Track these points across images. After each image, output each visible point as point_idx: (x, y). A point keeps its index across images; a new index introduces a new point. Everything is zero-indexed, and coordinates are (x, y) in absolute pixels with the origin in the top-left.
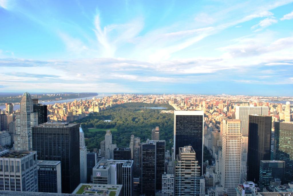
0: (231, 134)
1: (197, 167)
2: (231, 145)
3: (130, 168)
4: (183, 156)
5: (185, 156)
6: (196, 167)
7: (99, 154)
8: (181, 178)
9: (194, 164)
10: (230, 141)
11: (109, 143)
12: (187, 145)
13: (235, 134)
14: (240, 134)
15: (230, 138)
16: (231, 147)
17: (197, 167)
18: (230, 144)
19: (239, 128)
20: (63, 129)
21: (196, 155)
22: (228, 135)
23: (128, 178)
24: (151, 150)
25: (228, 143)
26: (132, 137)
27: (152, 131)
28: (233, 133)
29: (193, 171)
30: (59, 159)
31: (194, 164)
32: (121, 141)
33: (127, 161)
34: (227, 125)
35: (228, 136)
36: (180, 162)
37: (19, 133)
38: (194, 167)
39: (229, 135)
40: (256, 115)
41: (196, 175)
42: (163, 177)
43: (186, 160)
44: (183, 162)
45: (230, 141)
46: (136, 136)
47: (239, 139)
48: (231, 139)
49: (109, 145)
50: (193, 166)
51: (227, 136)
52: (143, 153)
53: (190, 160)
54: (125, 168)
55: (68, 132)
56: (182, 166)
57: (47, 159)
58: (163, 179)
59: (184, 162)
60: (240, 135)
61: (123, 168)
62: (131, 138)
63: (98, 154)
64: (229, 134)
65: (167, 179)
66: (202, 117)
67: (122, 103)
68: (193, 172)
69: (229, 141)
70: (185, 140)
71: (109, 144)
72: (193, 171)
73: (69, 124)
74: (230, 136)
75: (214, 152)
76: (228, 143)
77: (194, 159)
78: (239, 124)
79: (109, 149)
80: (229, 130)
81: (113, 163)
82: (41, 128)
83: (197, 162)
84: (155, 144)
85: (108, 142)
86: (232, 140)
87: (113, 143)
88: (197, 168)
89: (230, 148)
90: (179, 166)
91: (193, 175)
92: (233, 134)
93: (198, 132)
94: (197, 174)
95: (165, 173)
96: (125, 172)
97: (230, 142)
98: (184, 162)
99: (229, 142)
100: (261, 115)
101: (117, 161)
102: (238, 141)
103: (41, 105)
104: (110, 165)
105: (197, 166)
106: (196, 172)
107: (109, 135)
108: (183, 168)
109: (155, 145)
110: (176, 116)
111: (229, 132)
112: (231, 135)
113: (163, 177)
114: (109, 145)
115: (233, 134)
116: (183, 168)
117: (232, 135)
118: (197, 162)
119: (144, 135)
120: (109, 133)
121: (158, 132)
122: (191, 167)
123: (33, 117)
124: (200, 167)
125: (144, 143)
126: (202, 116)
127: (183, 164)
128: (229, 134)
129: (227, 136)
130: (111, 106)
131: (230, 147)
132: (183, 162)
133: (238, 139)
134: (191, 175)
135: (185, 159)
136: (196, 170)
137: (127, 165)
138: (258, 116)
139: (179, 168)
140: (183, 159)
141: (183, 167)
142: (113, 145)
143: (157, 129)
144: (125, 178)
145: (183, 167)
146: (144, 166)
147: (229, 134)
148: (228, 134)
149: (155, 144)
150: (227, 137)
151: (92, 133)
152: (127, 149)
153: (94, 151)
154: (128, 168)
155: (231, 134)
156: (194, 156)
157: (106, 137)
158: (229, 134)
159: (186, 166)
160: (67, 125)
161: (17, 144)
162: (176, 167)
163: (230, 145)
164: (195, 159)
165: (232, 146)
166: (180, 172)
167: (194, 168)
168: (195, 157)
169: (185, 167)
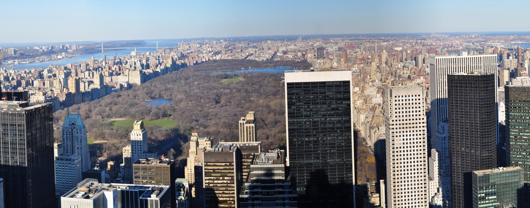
0: (401, 118)
1: (290, 196)
2: (404, 143)
4: (255, 172)
6: (287, 196)
9: (281, 190)
10: (400, 136)
11: (139, 149)
13: (411, 118)
14: (421, 117)
15: (400, 128)
16: (404, 147)
17: (290, 196)
18: (402, 142)
19: (419, 105)
22: (395, 123)
24: (223, 164)
25: (397, 140)
28: (406, 116)
31: (281, 190)
34: (394, 99)
35: (396, 125)
38: (281, 196)
39: (398, 122)
40: (463, 74)
45: (402, 134)
47: (420, 129)
48: (403, 130)
49: (140, 154)
51: (393, 125)
52: (207, 171)
60: (423, 119)
64: (398, 119)
69: (398, 134)
71: (139, 152)
74: (400, 124)
76: (397, 140)
78: (419, 95)
80: (398, 111)
85: (137, 147)
86: (405, 134)
88: (290, 199)
89: (402, 149)
92: (408, 118)
93: (340, 119)
97: (402, 138)
99: (399, 138)
100: (472, 73)
102: (419, 133)
105: (290, 193)
108: (257, 199)
111: (398, 115)
112: (401, 122)
115: (406, 118)
116: (257, 199)
117: (405, 122)
122: (276, 196)
128: (396, 119)
129: (393, 125)
131: (400, 148)
133: (418, 129)
136: (287, 201)
138: (466, 74)
147: (398, 119)
148: (395, 119)
150: (395, 127)
155: (401, 118)
156: (280, 172)
158: (396, 119)
163: (400, 144)
164: (284, 178)
165: (405, 145)
167: (284, 199)
168: (284, 172)
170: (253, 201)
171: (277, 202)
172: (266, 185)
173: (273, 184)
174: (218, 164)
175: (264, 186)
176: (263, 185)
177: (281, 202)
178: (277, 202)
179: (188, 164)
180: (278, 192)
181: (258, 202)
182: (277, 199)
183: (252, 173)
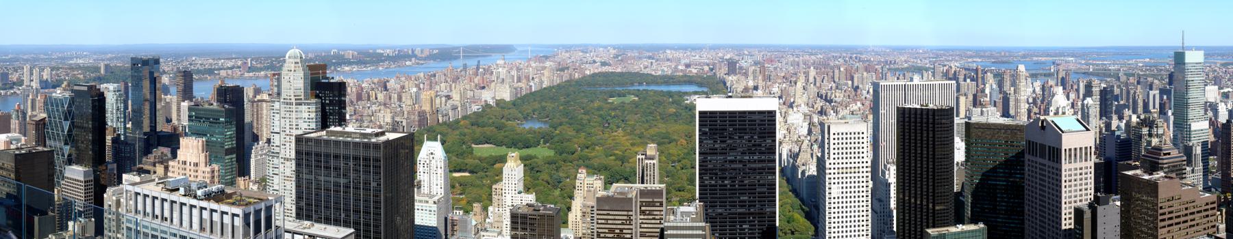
26: (582, 174)
30: (347, 224)
46: (594, 170)
57: (327, 221)
82: (318, 141)
87: (527, 189)
110: (701, 113)
143: (652, 149)
149: (632, 195)
160: (383, 134)
179: (573, 208)
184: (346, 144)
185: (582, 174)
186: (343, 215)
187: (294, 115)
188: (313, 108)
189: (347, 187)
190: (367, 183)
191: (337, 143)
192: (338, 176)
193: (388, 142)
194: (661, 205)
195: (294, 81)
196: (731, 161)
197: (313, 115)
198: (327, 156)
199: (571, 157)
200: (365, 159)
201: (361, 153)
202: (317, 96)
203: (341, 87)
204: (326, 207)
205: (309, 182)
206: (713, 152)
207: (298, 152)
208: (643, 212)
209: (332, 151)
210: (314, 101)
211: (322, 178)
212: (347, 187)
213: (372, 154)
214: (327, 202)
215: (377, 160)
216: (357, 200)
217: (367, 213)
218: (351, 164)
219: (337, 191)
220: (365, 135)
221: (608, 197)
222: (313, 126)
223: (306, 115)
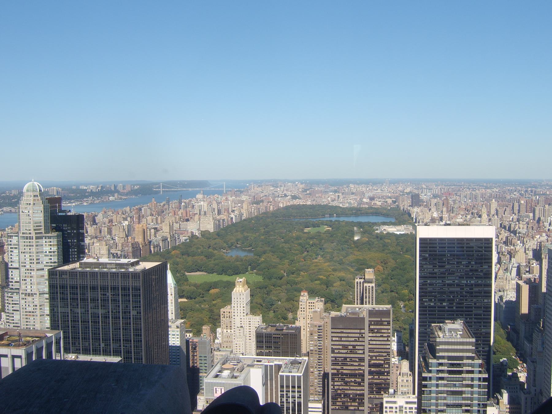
1: (480, 376)
3: (299, 377)
4: (441, 347)
5: (446, 347)
7: (216, 341)
8: (437, 405)
11: (242, 311)
12: (453, 319)
17: (480, 376)
20: (125, 275)
21: (477, 345)
23: (294, 403)
26: (304, 297)
27: (356, 280)
29: (467, 386)
31: (470, 369)
32: (274, 307)
33: (294, 358)
36: (434, 361)
37: (16, 286)
41: (476, 396)
42: (387, 402)
43: (450, 358)
44: (441, 361)
46: (313, 293)
49: (242, 317)
50: (468, 372)
53: (461, 358)
54: (288, 377)
55: (140, 283)
56: (439, 371)
58: (386, 407)
59: (445, 361)
61: (282, 377)
62: (301, 298)
63: (214, 341)
65: (396, 408)
66: (491, 243)
67: (273, 208)
68: (469, 389)
70: (444, 304)
72: (467, 386)
73: (140, 263)
75: (522, 334)
77: (470, 354)
79: (242, 327)
81: (256, 363)
82: (72, 273)
83: (480, 361)
84: (365, 314)
85: (239, 308)
88: (480, 379)
90: (430, 372)
91: (469, 396)
94: (479, 393)
95: (391, 391)
96: (288, 387)
98: (445, 361)
101: (264, 359)
103: (69, 214)
104: (248, 368)
105: (480, 372)
106: (476, 389)
107: (243, 292)
108: (442, 379)
109: (363, 319)
110: (421, 239)
113: (387, 402)
114: (242, 317)
116: (442, 379)
118: (480, 361)
119: (333, 293)
120: (243, 286)
121: (371, 282)
123: (51, 245)
124: (486, 376)
125: (334, 314)
126: (492, 239)
127: (441, 368)
130: (245, 215)
132: (441, 361)
134: (464, 396)
135: (446, 354)
136: (476, 382)
137: (293, 370)
139: (430, 378)
140: (441, 354)
141: (441, 375)
142: (254, 317)
144: (288, 403)
145: (441, 375)
146: (335, 371)
151: (195, 285)
152: (292, 328)
153: (204, 331)
154: (293, 377)
156: (470, 347)
157: (233, 296)
159: (450, 372)
160: (137, 263)
161: (13, 314)
162: (424, 375)
164: (473, 355)
166: (434, 389)
167: (472, 379)
169: (445, 375)
170: (437, 381)
171: (464, 382)
172: (453, 362)
173: (461, 362)
174: (344, 331)
175: (450, 364)
176: (450, 362)
177: (470, 382)
178: (464, 382)
180: (467, 371)
181: (443, 382)
182: (464, 379)
183: (438, 347)
184: (104, 275)
185: (304, 297)
186: (102, 345)
187: (34, 249)
188: (54, 241)
189: (106, 317)
190: (126, 312)
191: (94, 274)
192: (96, 307)
193: (145, 272)
194: (389, 324)
195: (33, 214)
196: (449, 285)
197: (55, 249)
198: (84, 287)
199: (279, 282)
200: (124, 289)
201: (120, 283)
202: (57, 229)
203: (79, 220)
204: (84, 339)
205: (65, 315)
206: (433, 276)
207: (52, 287)
208: (371, 331)
209: (89, 282)
210: (55, 234)
211: (79, 310)
212: (106, 317)
213: (131, 283)
214: (85, 333)
215: (137, 289)
216: (117, 329)
217: (127, 340)
218: (109, 294)
219: (95, 322)
220: (121, 265)
221: (341, 316)
222: (55, 259)
223: (47, 249)
